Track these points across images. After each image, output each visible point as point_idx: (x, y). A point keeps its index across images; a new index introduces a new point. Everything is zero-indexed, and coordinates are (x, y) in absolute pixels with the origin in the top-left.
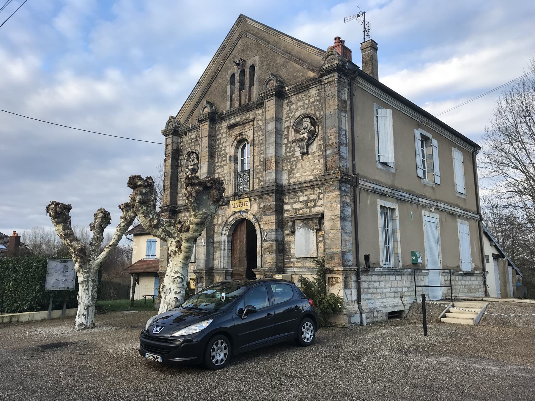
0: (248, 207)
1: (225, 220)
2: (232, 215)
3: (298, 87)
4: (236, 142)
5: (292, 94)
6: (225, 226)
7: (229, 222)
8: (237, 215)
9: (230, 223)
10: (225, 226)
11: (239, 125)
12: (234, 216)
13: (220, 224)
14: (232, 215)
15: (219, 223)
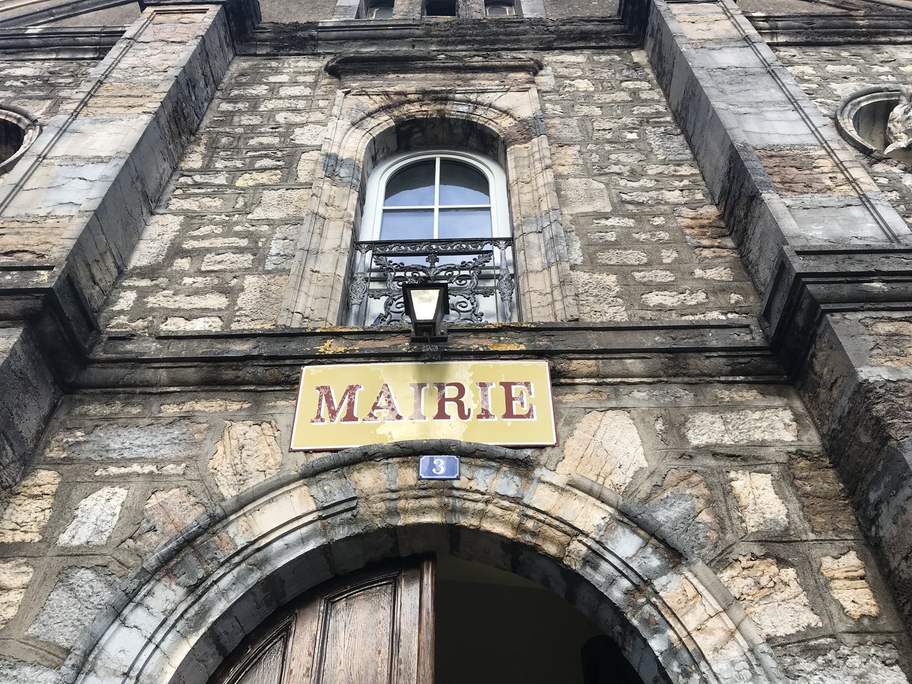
0: (537, 429)
1: (179, 511)
2: (310, 475)
3: (819, 22)
4: (385, 122)
5: (781, 39)
6: (166, 566)
7: (238, 533)
8: (368, 479)
9: (253, 552)
10: (166, 566)
11: (425, 70)
12: (333, 489)
13: (78, 556)
14: (310, 475)
15: (76, 534)
